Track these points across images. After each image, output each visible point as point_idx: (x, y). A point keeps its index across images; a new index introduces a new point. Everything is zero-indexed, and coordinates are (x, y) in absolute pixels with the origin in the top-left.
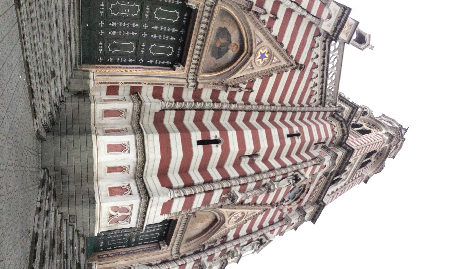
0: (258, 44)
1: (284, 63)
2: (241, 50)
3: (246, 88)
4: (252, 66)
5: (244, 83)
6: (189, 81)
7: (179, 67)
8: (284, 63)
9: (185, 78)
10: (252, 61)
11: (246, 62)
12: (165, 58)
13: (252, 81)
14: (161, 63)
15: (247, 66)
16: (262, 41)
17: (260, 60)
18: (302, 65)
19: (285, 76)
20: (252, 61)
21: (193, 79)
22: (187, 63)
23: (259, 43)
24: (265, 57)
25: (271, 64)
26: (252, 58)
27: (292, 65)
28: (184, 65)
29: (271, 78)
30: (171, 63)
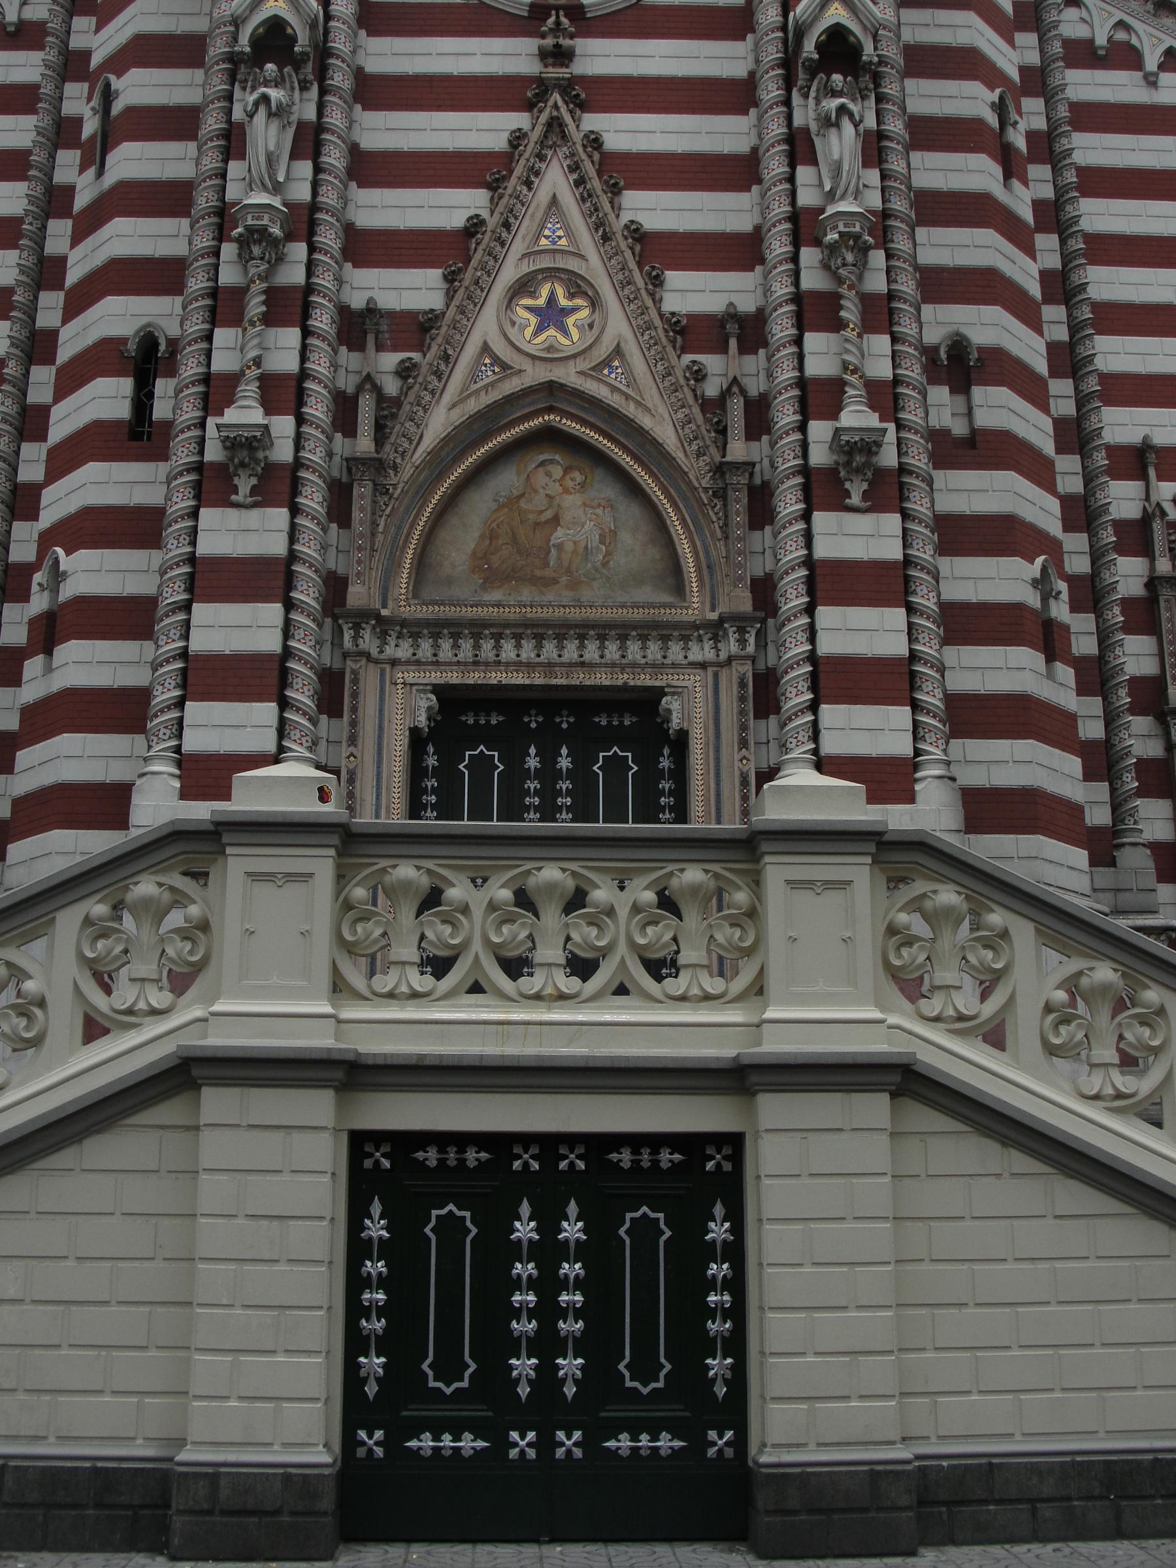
0: (505, 366)
1: (555, 179)
2: (550, 437)
3: (723, 349)
4: (606, 363)
5: (698, 375)
6: (723, 656)
7: (669, 711)
8: (555, 179)
9: (716, 676)
10: (581, 373)
11: (594, 403)
13: (682, 332)
15: (614, 389)
16: (486, 348)
17: (570, 321)
18: (544, 55)
19: (628, 132)
20: (581, 373)
21: (715, 638)
22: (645, 680)
23: (496, 360)
24: (552, 299)
25: (582, 257)
26: (568, 375)
27: (555, 126)
28: (660, 692)
29: (652, 222)
30: (666, 751)
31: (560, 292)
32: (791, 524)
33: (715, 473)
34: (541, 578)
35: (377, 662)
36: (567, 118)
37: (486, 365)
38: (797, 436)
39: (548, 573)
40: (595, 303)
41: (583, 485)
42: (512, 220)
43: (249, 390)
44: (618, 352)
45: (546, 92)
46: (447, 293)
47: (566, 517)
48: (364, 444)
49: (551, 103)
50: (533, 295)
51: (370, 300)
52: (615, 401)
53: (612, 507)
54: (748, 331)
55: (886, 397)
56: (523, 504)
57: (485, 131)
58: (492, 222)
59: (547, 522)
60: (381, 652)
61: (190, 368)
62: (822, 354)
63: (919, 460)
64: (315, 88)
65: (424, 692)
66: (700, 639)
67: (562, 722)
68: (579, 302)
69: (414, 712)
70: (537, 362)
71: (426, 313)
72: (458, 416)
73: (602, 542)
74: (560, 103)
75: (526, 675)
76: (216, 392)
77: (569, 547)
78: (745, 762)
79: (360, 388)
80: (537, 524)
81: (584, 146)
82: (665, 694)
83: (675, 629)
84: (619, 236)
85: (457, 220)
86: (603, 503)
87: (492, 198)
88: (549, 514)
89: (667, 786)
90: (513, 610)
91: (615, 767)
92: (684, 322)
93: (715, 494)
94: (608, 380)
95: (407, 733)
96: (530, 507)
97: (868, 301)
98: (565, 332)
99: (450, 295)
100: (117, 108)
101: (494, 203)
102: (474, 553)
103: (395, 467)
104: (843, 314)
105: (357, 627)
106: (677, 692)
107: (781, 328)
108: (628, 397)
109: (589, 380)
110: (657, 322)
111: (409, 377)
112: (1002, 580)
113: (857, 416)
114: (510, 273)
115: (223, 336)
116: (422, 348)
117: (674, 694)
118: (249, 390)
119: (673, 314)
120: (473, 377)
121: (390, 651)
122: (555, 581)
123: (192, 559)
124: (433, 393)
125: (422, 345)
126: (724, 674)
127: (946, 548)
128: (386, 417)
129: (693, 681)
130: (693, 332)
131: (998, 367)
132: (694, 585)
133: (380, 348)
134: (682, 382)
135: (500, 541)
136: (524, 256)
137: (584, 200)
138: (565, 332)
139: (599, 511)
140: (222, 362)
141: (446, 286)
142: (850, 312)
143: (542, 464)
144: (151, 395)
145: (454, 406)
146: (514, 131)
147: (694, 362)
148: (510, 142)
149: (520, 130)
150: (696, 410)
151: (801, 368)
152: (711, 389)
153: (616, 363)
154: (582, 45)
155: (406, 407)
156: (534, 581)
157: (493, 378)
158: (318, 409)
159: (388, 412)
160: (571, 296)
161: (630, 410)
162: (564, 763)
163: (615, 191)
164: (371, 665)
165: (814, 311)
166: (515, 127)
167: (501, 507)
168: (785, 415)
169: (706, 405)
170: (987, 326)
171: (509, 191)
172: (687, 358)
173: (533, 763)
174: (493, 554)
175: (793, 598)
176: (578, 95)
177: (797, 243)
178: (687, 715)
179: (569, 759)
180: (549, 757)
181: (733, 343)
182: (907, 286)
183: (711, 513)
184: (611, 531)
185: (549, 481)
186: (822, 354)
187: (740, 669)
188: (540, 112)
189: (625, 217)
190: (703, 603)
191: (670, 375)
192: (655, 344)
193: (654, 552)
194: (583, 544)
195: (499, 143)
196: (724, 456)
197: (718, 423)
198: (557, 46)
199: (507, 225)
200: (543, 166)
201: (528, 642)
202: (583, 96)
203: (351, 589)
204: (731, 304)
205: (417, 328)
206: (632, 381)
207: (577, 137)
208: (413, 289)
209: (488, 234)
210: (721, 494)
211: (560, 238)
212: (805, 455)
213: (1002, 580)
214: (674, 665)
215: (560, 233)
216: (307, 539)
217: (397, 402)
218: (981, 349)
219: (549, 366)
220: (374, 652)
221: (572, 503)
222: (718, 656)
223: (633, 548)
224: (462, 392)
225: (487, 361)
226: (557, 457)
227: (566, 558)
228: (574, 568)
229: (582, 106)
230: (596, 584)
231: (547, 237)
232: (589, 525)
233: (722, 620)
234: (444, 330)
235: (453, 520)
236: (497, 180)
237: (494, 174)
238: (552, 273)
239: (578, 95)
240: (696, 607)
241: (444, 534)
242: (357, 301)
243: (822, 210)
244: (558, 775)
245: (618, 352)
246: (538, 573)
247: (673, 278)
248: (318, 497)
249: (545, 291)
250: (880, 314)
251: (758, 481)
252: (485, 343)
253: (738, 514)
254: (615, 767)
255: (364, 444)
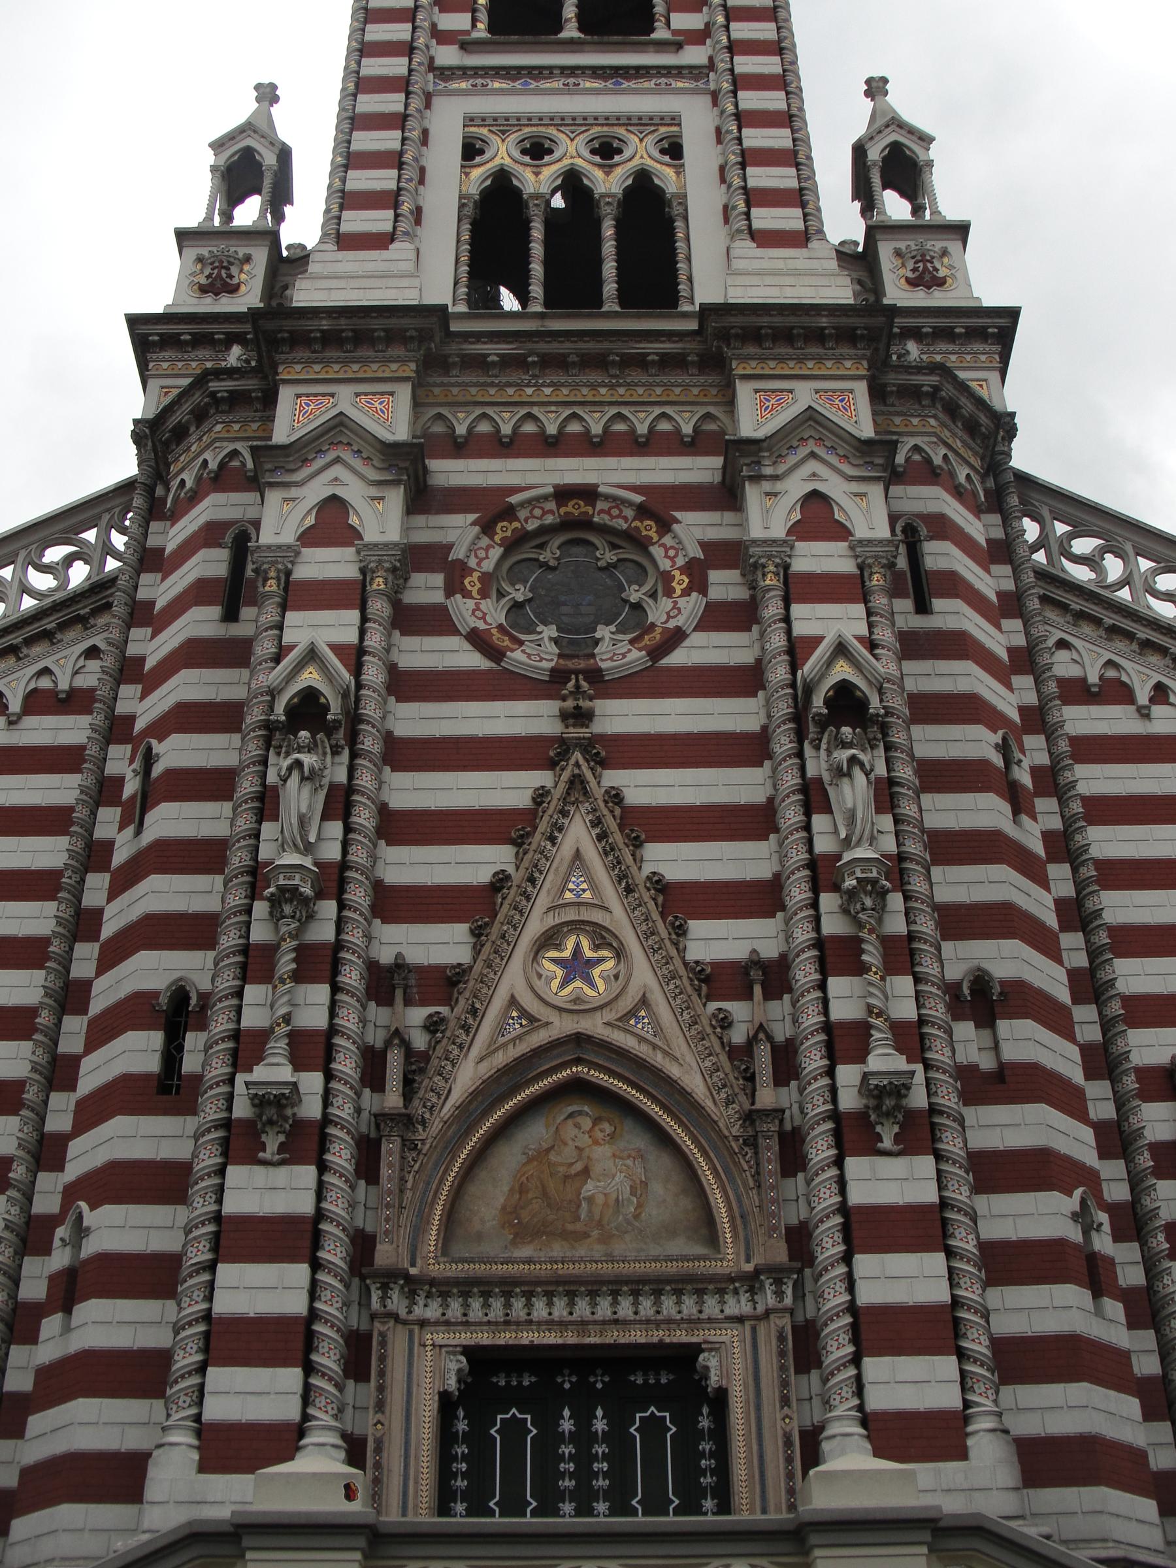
0: (532, 1019)
1: (577, 833)
2: (579, 1088)
3: (749, 996)
4: (632, 1013)
5: (724, 1022)
6: (760, 1309)
7: (707, 1368)
8: (577, 833)
9: (754, 1330)
10: (608, 1024)
11: (622, 1054)
12: (688, 1438)
13: (707, 980)
14: (712, 1455)
15: (641, 1039)
16: (513, 1002)
17: (596, 972)
18: (564, 716)
19: (647, 787)
20: (608, 1024)
21: (752, 1291)
22: (681, 1336)
23: (524, 1013)
24: (577, 951)
25: (606, 909)
26: (594, 1025)
27: (577, 783)
28: (695, 1350)
29: (674, 873)
30: (705, 1410)
31: (585, 944)
32: (823, 1170)
33: (745, 1121)
34: (572, 1232)
35: (405, 1323)
36: (588, 775)
37: (513, 1018)
38: (826, 1081)
39: (579, 1227)
40: (620, 954)
41: (612, 1136)
42: (536, 875)
43: (278, 1046)
44: (644, 1002)
45: (567, 751)
46: (474, 948)
47: (596, 1169)
48: (393, 1099)
49: (572, 761)
50: (558, 947)
51: (399, 955)
52: (642, 1050)
53: (642, 1157)
54: (772, 977)
55: (912, 1038)
56: (553, 1157)
57: (510, 789)
58: (517, 877)
59: (577, 1174)
60: (410, 1312)
61: (221, 1024)
62: (846, 998)
63: (948, 1099)
64: (346, 751)
65: (454, 1353)
66: (736, 1292)
67: (596, 1382)
68: (604, 953)
69: (443, 1379)
70: (564, 1015)
71: (453, 967)
72: (486, 1069)
73: (633, 1193)
74: (581, 761)
75: (559, 1334)
76: (246, 1048)
77: (600, 1199)
78: (787, 1421)
79: (388, 1043)
80: (566, 1177)
81: (606, 802)
82: (703, 1351)
83: (710, 1283)
84: (641, 888)
85: (483, 876)
86: (633, 1154)
87: (517, 853)
88: (579, 1167)
89: (708, 1447)
90: (544, 1267)
91: (652, 1428)
92: (709, 970)
93: (745, 1143)
94: (635, 1030)
95: (436, 1398)
96: (559, 1159)
97: (887, 942)
98: (591, 984)
99: (477, 950)
100: (157, 770)
101: (519, 859)
102: (504, 1208)
103: (423, 1122)
104: (865, 957)
105: (385, 1287)
106: (715, 1348)
107: (805, 973)
108: (655, 1047)
109: (616, 1031)
110: (682, 971)
111: (437, 1031)
112: (1041, 1216)
113: (884, 1059)
114: (535, 926)
115: (254, 993)
116: (449, 1001)
117: (711, 1350)
118: (278, 1046)
119: (697, 963)
120: (501, 1030)
121: (418, 1311)
122: (586, 1235)
123: (218, 1218)
124: (461, 1047)
125: (451, 999)
126: (762, 1329)
127: (982, 1186)
128: (414, 1072)
129: (729, 1335)
130: (719, 980)
131: (1021, 1000)
132: (728, 1235)
133: (408, 1002)
134: (709, 1030)
135: (530, 1196)
136: (549, 909)
137: (606, 854)
138: (591, 984)
139: (629, 1162)
140: (252, 1019)
141: (473, 940)
142: (872, 955)
143: (571, 1116)
144: (180, 1048)
145: (482, 1060)
146: (538, 789)
147: (720, 1010)
148: (533, 799)
149: (543, 787)
150: (724, 1058)
151: (826, 1011)
152: (738, 1036)
153: (643, 1013)
154: (603, 706)
155: (434, 1062)
156: (565, 1235)
157: (520, 1031)
158: (347, 1064)
159: (417, 1066)
160: (597, 948)
161: (658, 1059)
162: (600, 1425)
163: (636, 844)
164: (400, 1327)
165: (837, 956)
166: (538, 785)
167: (530, 1161)
168: (813, 1060)
169: (733, 1052)
170: (1009, 960)
171: (533, 847)
172: (713, 1006)
173: (567, 1426)
174: (522, 1208)
175: (829, 1246)
176: (598, 753)
177: (816, 890)
178: (726, 1373)
179: (605, 1421)
180: (583, 1419)
181: (758, 990)
182: (926, 926)
183: (742, 1161)
184: (641, 1182)
185: (577, 1133)
186: (846, 998)
187: (778, 1322)
188: (563, 770)
189: (647, 869)
190: (737, 1254)
191: (696, 1023)
192: (681, 993)
193: (686, 1203)
194: (614, 1196)
195: (522, 800)
196: (753, 1104)
197: (746, 1070)
198: (577, 707)
199: (532, 880)
200: (566, 822)
201: (560, 1299)
202: (603, 754)
203: (379, 1247)
204: (754, 951)
205: (445, 983)
206: (658, 1031)
207: (599, 793)
208: (441, 944)
209: (514, 889)
210: (752, 1142)
211: (584, 890)
212: (834, 1100)
213: (1041, 1216)
214: (710, 1320)
215: (584, 886)
216: (334, 1198)
217: (425, 1056)
218: (1003, 983)
219: (575, 1017)
220: (403, 1313)
221: (602, 1154)
222: (755, 1308)
223: (664, 1199)
224: (489, 1046)
225: (515, 1014)
226: (586, 1108)
227: (597, 1211)
228: (605, 1221)
229: (604, 764)
230: (628, 1237)
231: (571, 891)
232: (619, 1177)
233: (757, 1272)
234: (472, 983)
235: (482, 1174)
236: (522, 836)
237: (519, 830)
238: (577, 926)
239: (598, 753)
240: (730, 1259)
241: (472, 1189)
242: (386, 956)
243: (839, 857)
244: (593, 1438)
245: (644, 1002)
246: (570, 1227)
247: (697, 927)
248: (346, 1154)
249: (570, 943)
250: (902, 955)
251: (788, 1127)
252: (513, 996)
253: (769, 1161)
254: (652, 1428)
255: (393, 1099)
